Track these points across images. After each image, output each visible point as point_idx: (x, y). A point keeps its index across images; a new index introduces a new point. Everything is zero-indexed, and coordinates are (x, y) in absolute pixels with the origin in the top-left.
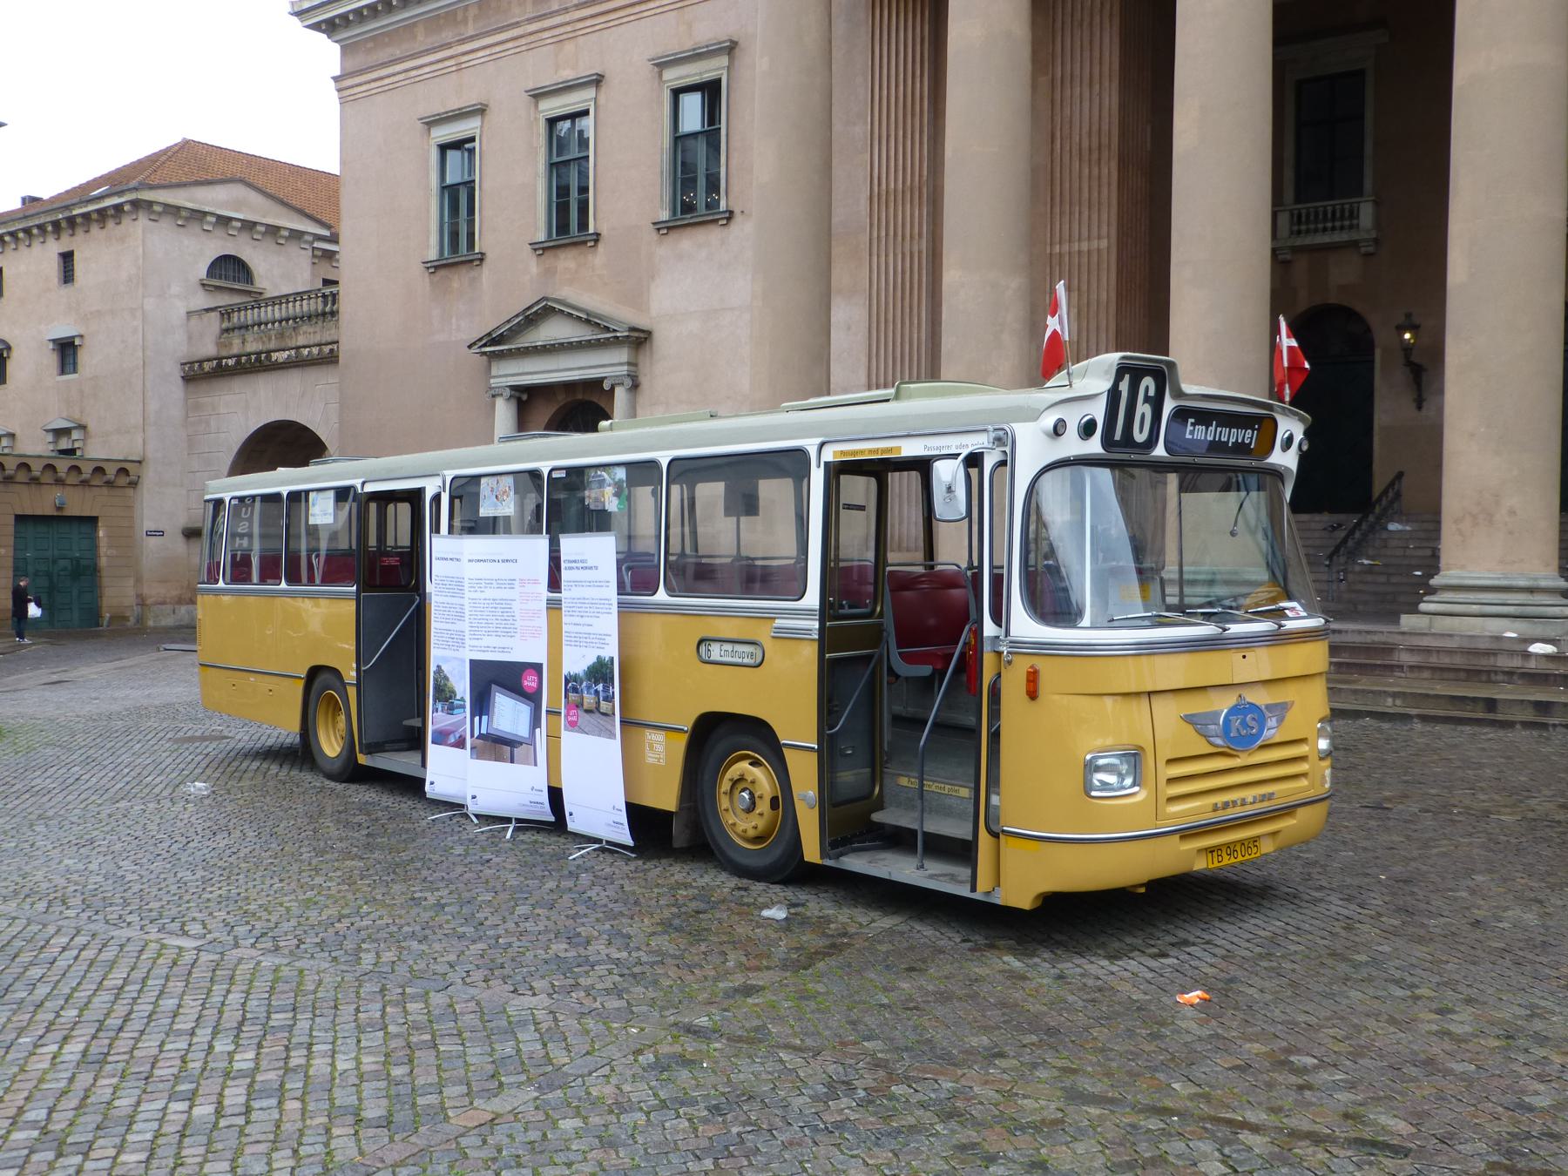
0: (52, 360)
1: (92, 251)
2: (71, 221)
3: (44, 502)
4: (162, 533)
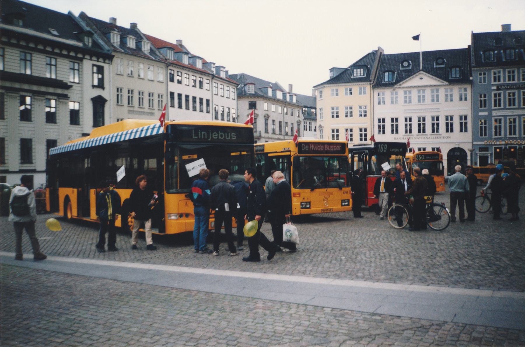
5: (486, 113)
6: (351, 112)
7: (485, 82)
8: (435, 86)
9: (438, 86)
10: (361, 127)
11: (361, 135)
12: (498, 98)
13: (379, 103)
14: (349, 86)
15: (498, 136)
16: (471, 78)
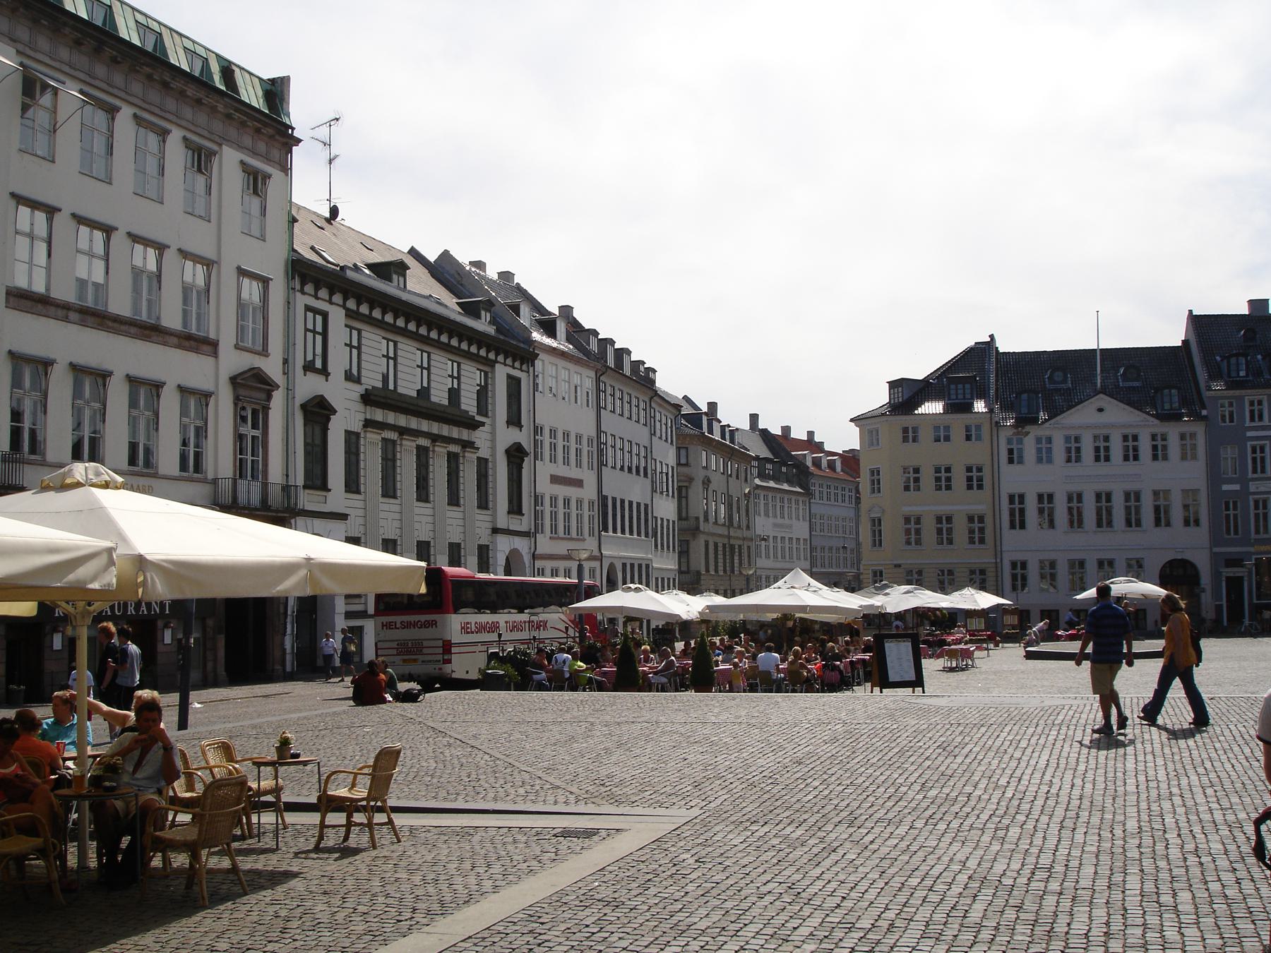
5: (1237, 487)
6: (948, 479)
7: (1231, 421)
8: (1131, 426)
11: (971, 531)
12: (1258, 455)
13: (1011, 461)
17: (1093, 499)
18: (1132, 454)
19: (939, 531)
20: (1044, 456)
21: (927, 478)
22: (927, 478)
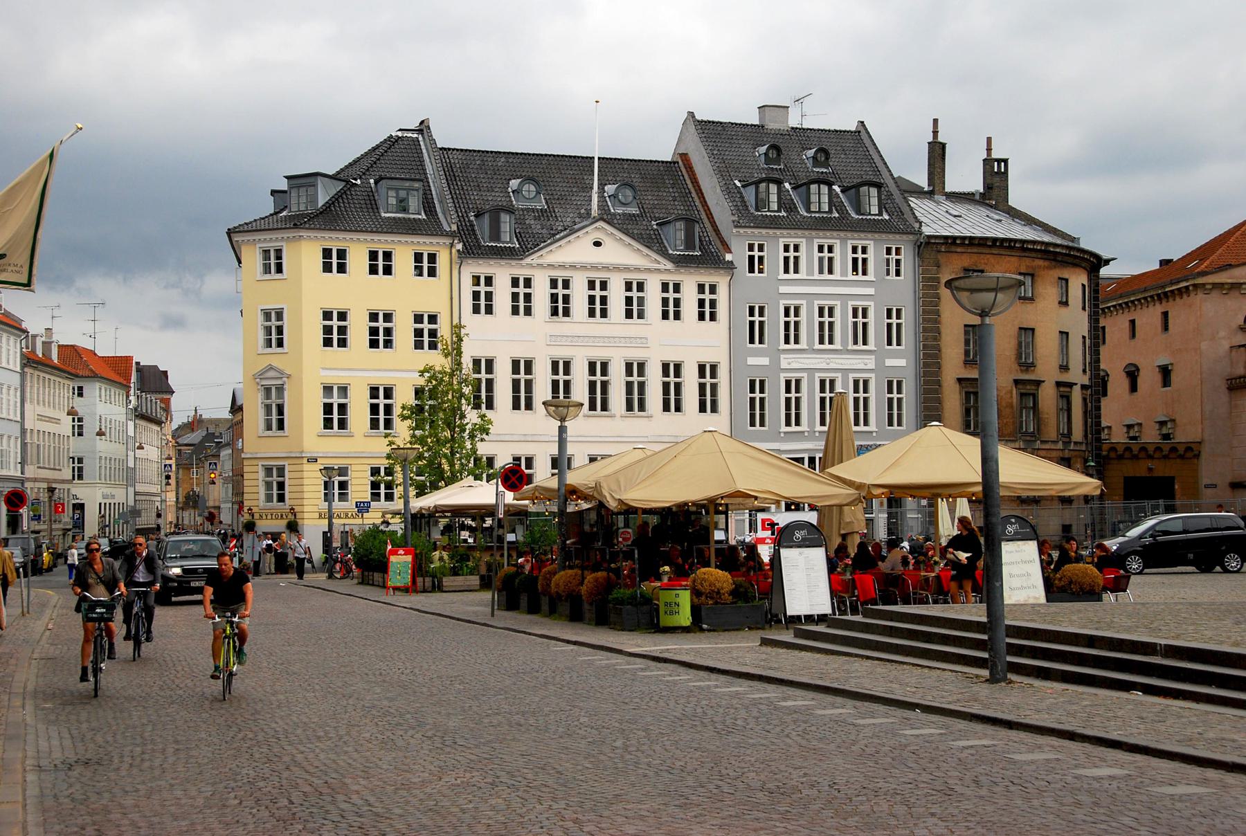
0: (1158, 377)
1: (1178, 311)
2: (1165, 294)
3: (1140, 469)
4: (1215, 486)
5: (765, 361)
8: (638, 270)
9: (649, 270)
10: (375, 382)
14: (382, 243)
15: (794, 428)
16: (728, 257)
17: (509, 367)
18: (634, 309)
19: (374, 409)
20: (522, 305)
21: (358, 330)
22: (358, 330)
